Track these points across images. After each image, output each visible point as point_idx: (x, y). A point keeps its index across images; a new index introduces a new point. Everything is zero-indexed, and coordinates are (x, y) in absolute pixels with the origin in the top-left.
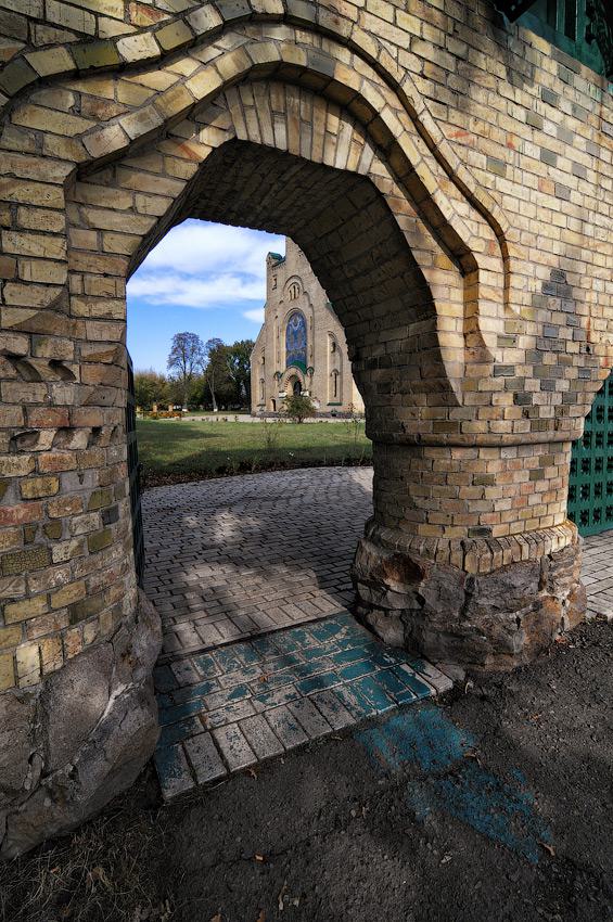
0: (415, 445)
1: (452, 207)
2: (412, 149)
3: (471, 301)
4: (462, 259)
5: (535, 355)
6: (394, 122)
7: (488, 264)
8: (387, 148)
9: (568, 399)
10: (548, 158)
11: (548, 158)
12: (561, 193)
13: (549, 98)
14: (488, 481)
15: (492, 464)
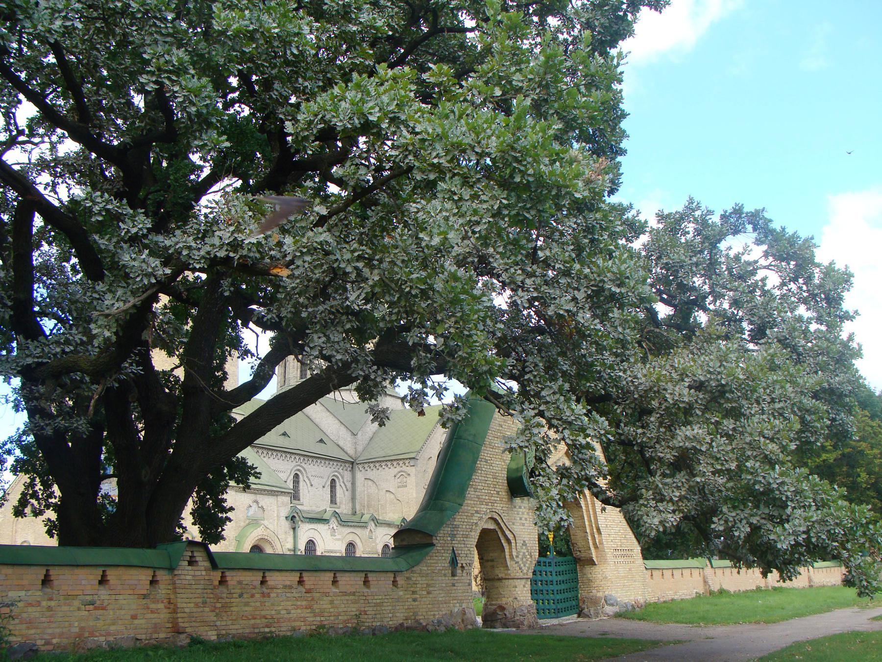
0: (500, 579)
1: (507, 532)
2: (502, 524)
3: (510, 548)
4: (509, 541)
5: (522, 559)
6: (500, 521)
7: (513, 541)
8: (498, 524)
9: (529, 568)
10: (521, 519)
11: (521, 519)
12: (523, 525)
13: (520, 507)
14: (516, 587)
15: (517, 582)
